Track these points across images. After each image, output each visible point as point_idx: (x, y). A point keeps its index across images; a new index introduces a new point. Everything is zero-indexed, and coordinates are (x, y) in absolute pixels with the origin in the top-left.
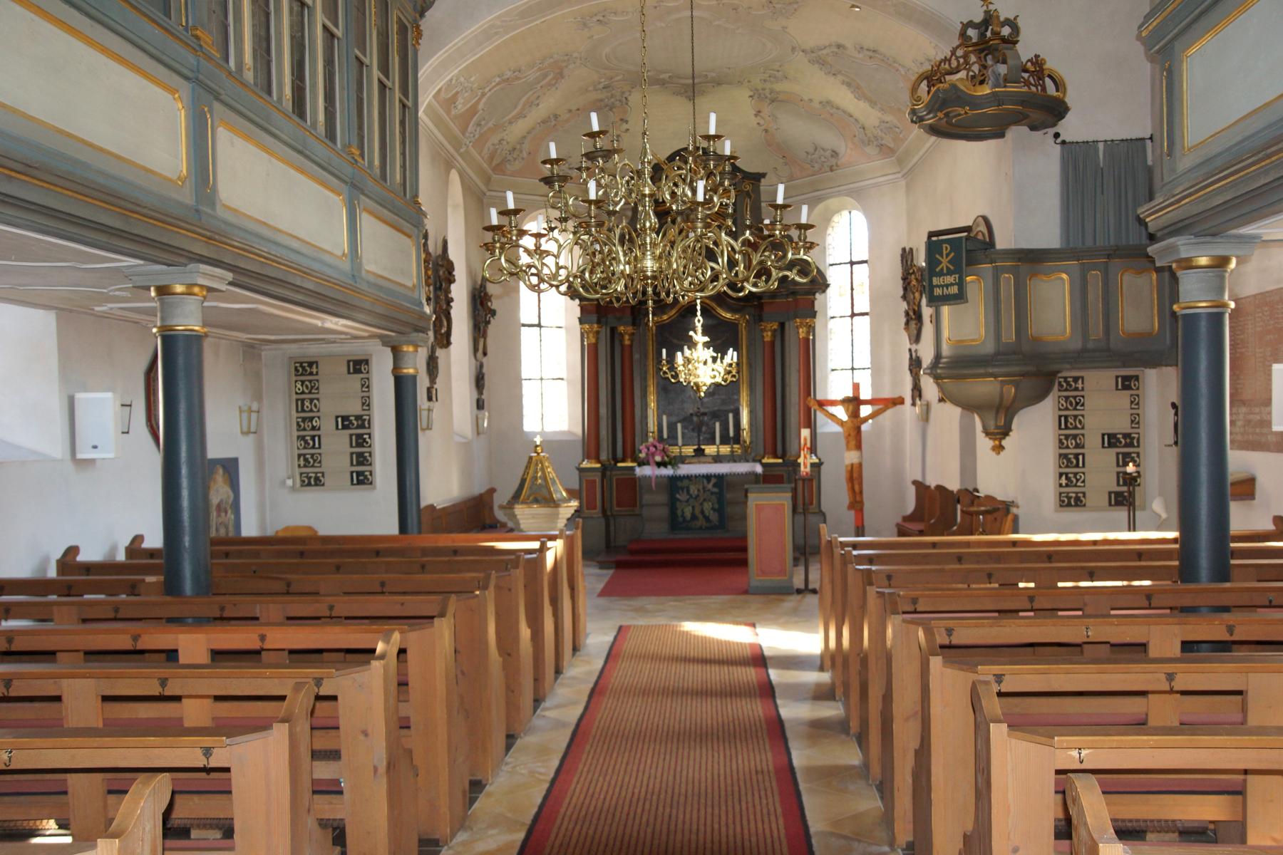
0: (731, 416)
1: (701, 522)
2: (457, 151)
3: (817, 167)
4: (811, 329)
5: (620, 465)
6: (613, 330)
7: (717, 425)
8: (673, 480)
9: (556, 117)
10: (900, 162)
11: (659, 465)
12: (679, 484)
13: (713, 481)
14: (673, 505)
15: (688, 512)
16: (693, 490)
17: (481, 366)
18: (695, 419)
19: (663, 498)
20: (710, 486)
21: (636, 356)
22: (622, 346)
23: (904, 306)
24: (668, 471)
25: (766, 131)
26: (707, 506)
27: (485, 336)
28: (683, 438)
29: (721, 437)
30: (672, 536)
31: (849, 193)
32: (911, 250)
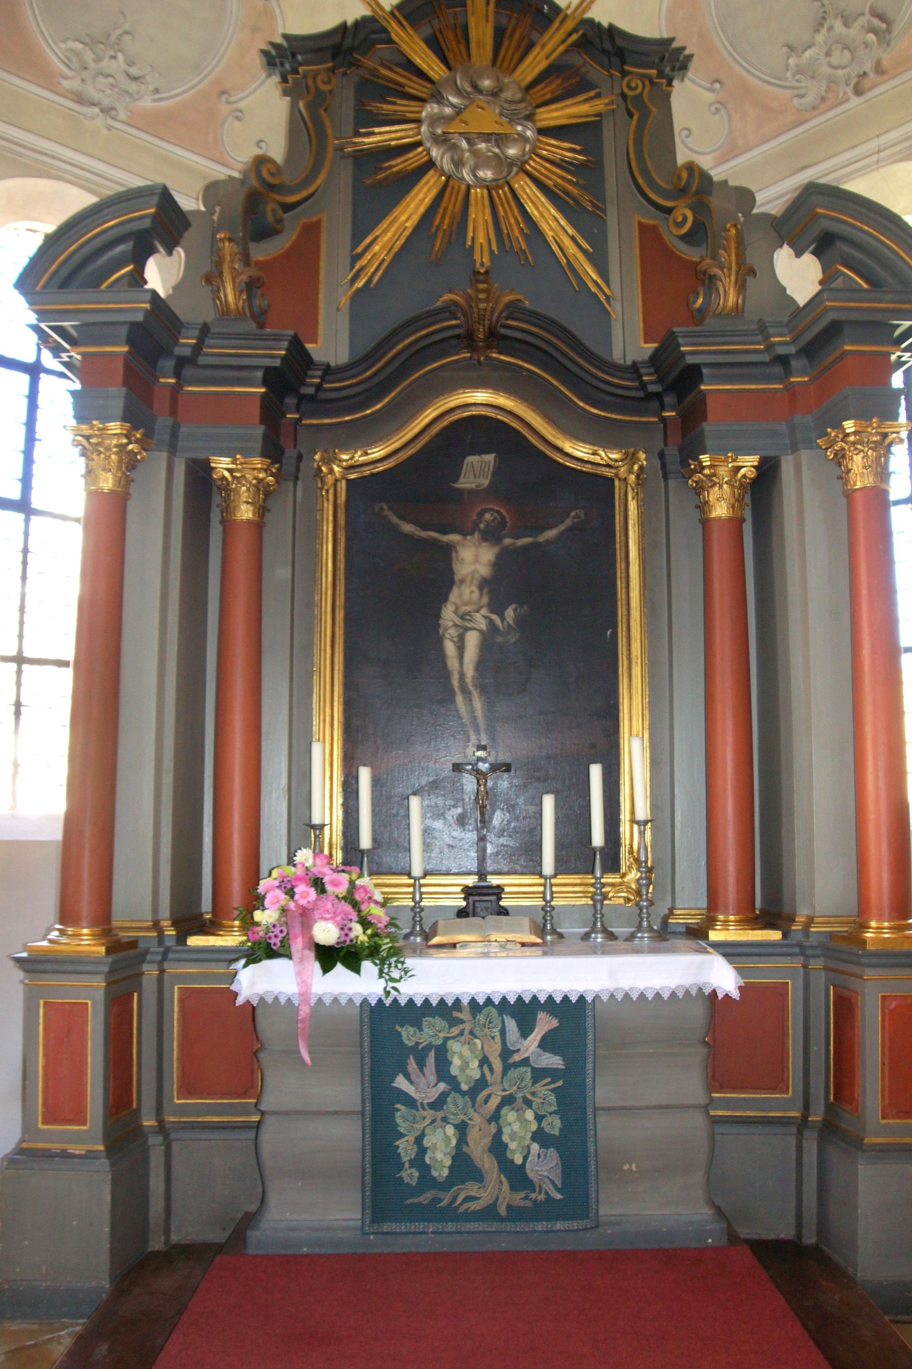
0: (596, 772)
1: (493, 1190)
3: (814, 90)
5: (195, 941)
7: (548, 802)
8: (385, 1022)
11: (328, 957)
12: (408, 1035)
13: (545, 1023)
14: (381, 1109)
15: (440, 1158)
16: (464, 1061)
18: (469, 783)
19: (345, 1091)
20: (530, 1046)
21: (278, 573)
22: (227, 523)
24: (365, 984)
26: (518, 1127)
28: (427, 847)
29: (559, 846)
30: (377, 1245)
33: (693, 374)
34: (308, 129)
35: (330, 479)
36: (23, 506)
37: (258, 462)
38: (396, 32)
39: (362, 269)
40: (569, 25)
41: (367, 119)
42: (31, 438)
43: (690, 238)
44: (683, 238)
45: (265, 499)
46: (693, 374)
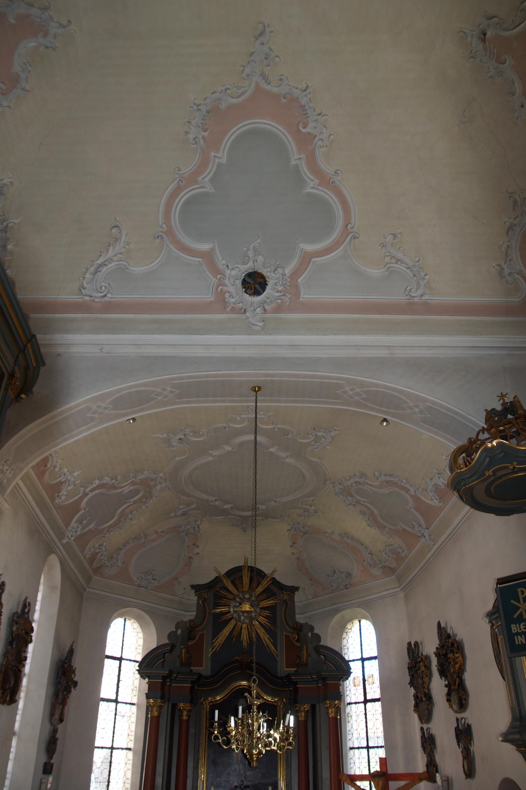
2: (60, 540)
4: (338, 710)
6: (174, 706)
9: (146, 536)
10: (399, 579)
17: (55, 731)
21: (192, 731)
22: (181, 720)
23: (412, 691)
25: (298, 559)
27: (64, 703)
31: (360, 605)
32: (416, 644)
33: (296, 683)
34: (202, 609)
35: (205, 706)
36: (116, 701)
37: (189, 705)
38: (225, 581)
39: (215, 646)
40: (269, 579)
41: (217, 605)
42: (119, 681)
43: (298, 641)
44: (296, 641)
45: (189, 711)
46: (296, 683)
